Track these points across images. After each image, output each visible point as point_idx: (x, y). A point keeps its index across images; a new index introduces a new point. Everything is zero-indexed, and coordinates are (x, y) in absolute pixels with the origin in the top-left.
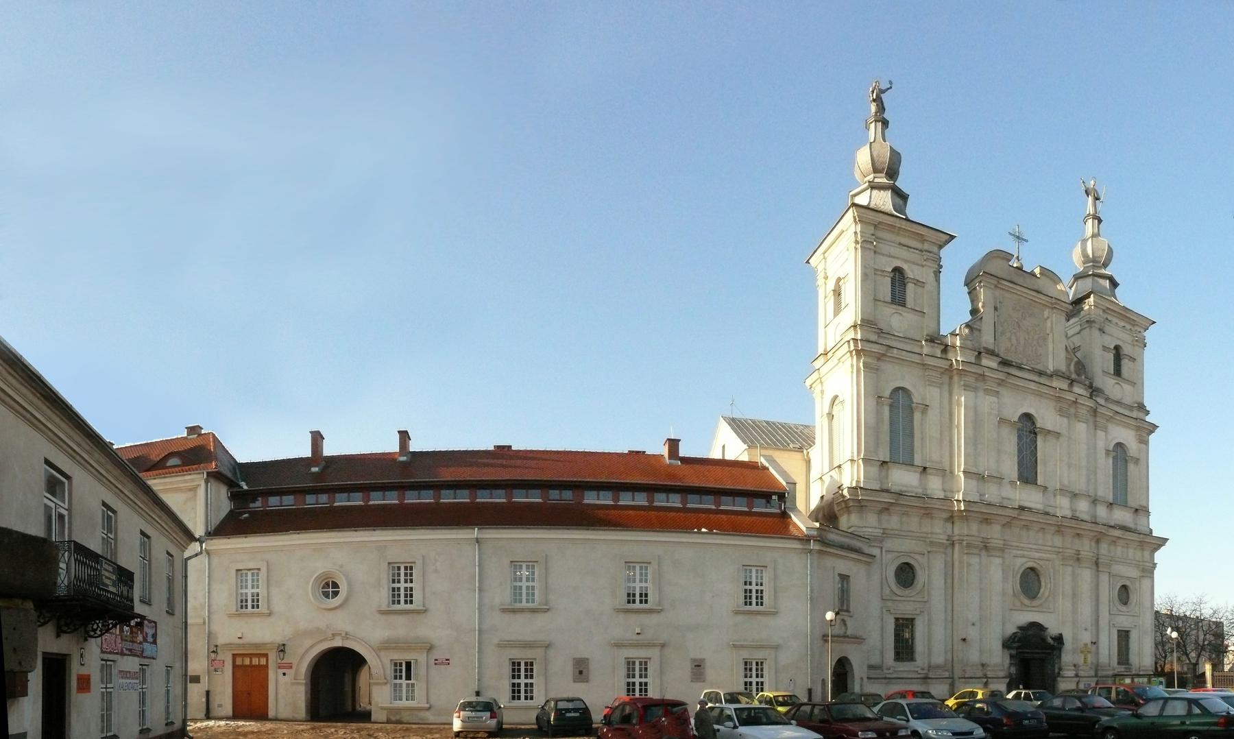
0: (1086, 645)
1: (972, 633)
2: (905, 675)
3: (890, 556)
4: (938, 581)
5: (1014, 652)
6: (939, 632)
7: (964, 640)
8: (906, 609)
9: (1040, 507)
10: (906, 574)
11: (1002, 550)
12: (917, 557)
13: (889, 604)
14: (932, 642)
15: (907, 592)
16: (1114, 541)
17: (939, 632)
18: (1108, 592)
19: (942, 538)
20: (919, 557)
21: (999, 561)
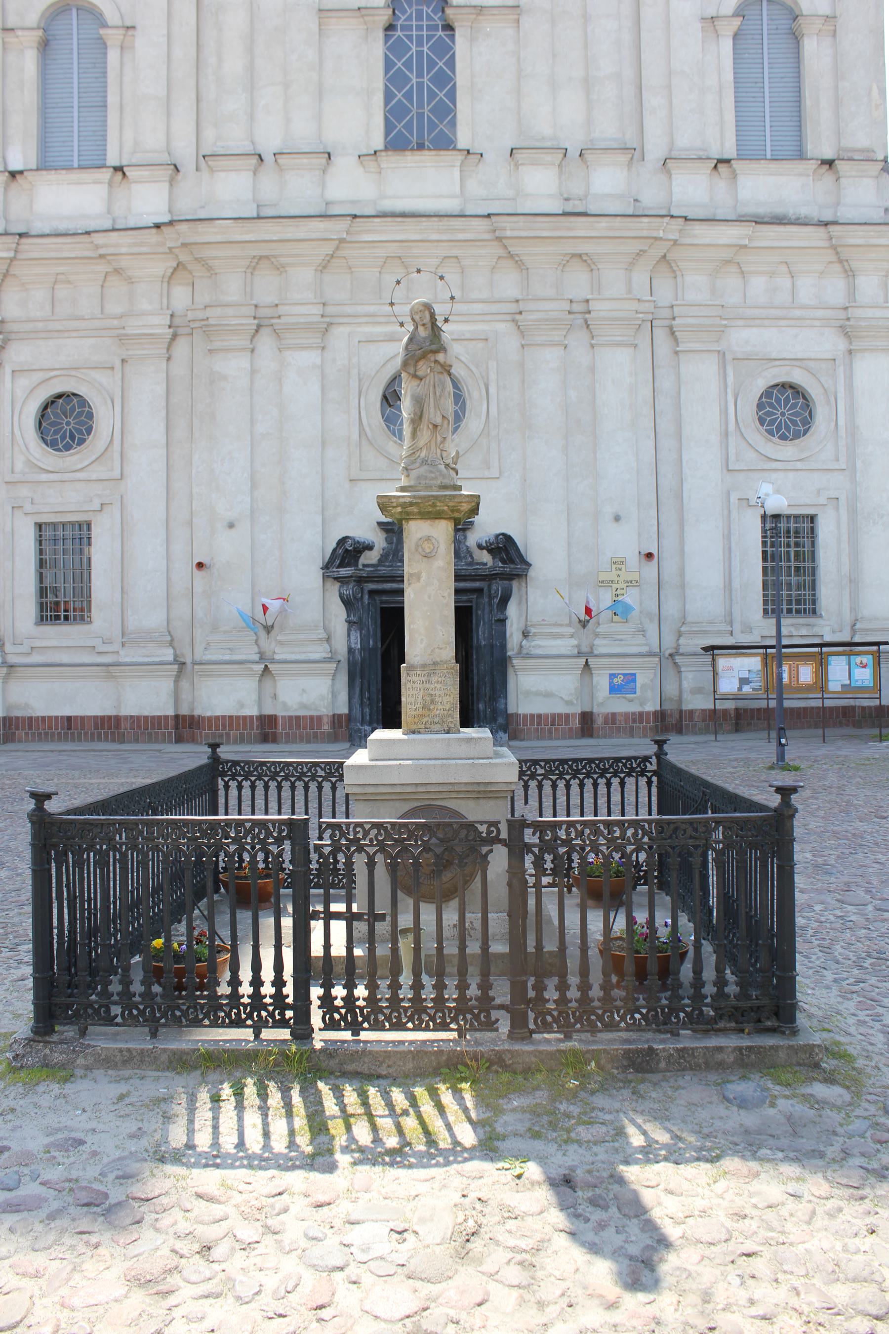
0: (618, 563)
1: (226, 548)
2: (65, 658)
3: (24, 383)
4: (146, 427)
5: (348, 591)
6: (149, 552)
7: (200, 565)
8: (64, 502)
9: (451, 205)
10: (64, 420)
11: (325, 328)
12: (96, 375)
13: (24, 491)
14: (129, 575)
15: (74, 459)
16: (733, 260)
17: (149, 552)
18: (710, 403)
19: (158, 324)
20: (99, 376)
21: (306, 358)
